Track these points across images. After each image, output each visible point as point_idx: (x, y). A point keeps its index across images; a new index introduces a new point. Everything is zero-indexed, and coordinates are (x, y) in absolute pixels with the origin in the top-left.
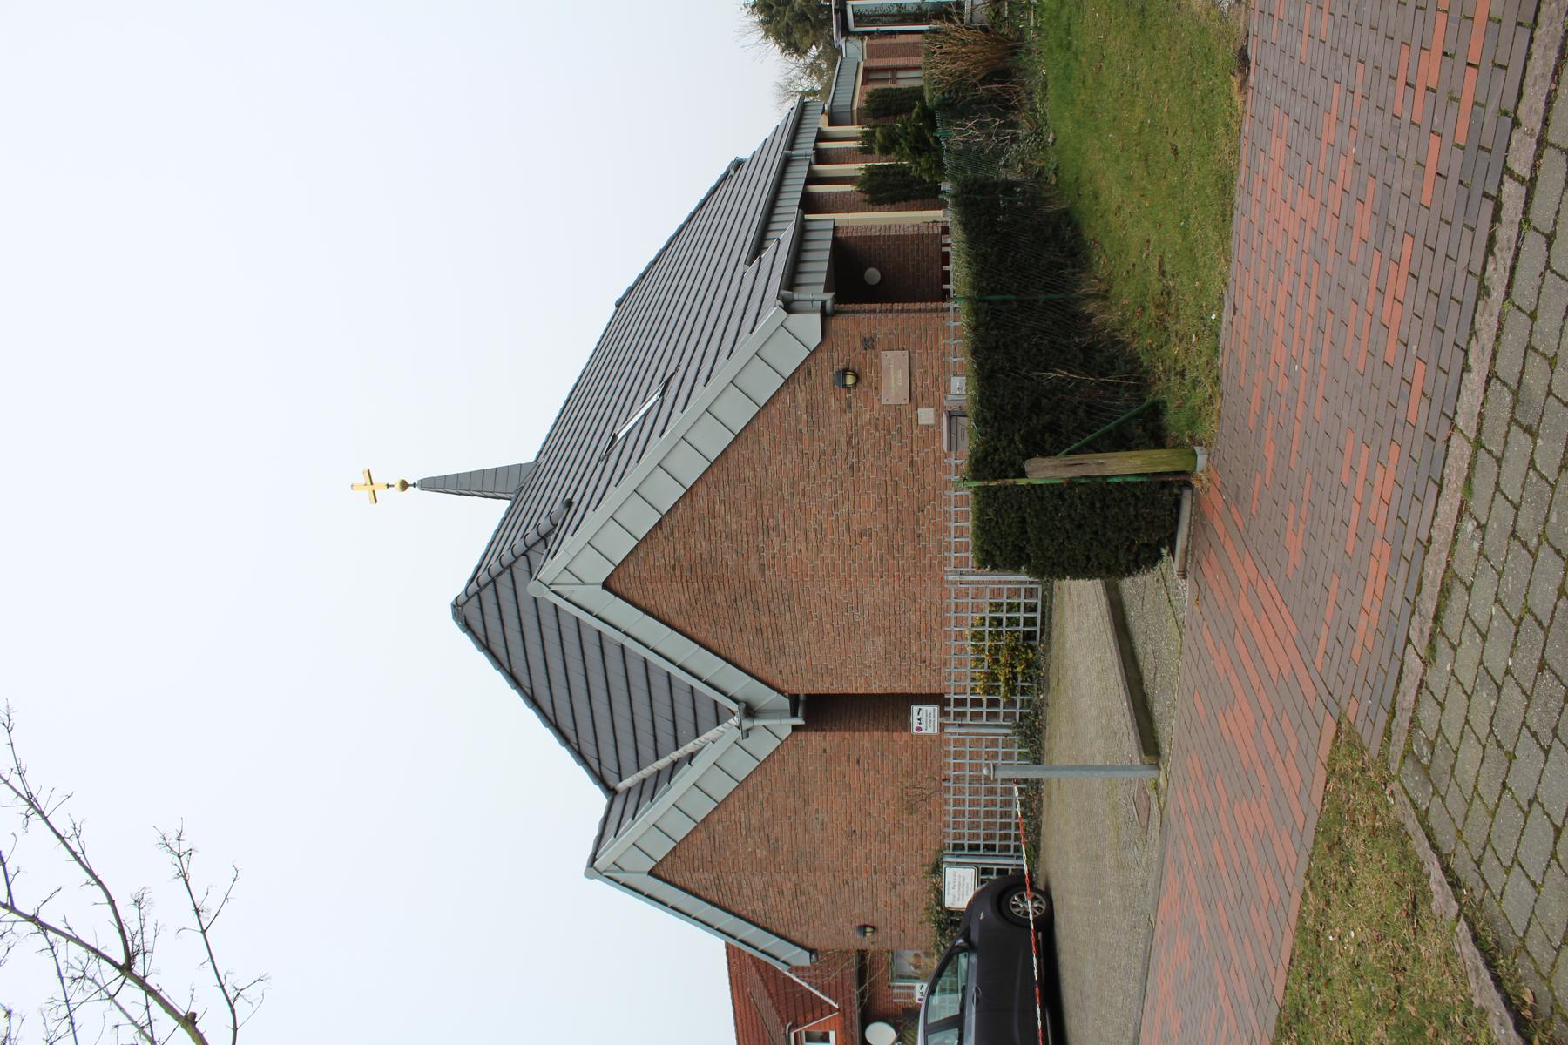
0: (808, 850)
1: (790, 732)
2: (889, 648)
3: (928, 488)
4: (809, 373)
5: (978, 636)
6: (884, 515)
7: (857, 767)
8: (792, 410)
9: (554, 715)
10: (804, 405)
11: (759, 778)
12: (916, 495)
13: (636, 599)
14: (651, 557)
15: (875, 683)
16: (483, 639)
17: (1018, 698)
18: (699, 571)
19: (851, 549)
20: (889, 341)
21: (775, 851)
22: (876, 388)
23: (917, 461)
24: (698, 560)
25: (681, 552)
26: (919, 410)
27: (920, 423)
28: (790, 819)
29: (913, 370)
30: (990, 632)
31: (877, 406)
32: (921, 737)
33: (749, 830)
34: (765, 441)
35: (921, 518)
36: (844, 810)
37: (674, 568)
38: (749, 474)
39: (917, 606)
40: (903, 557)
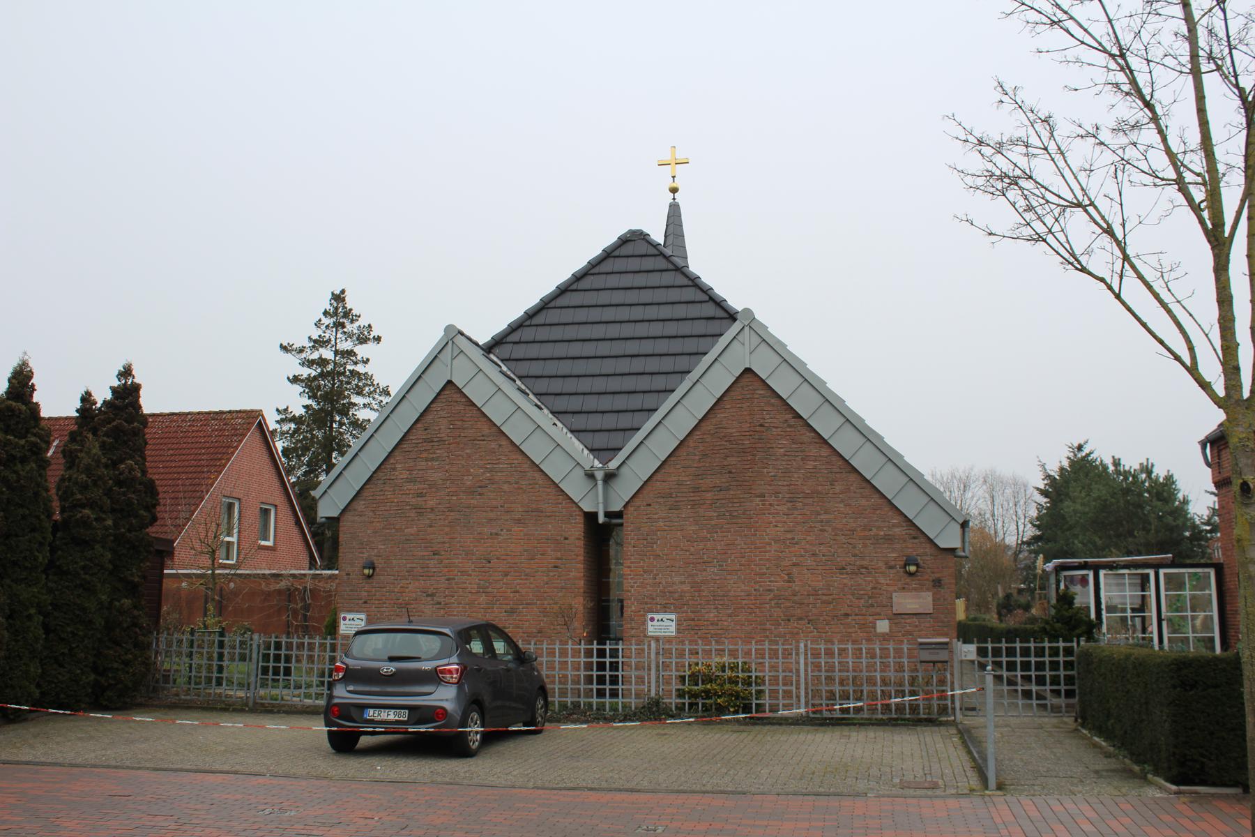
0: (471, 521)
1: (586, 510)
2: (676, 595)
3: (827, 627)
4: (914, 538)
5: (734, 668)
6: (805, 593)
7: (550, 566)
8: (887, 524)
9: (555, 308)
10: (890, 533)
11: (540, 482)
12: (822, 618)
13: (732, 393)
14: (770, 408)
15: (635, 583)
16: (616, 253)
17: (687, 701)
18: (760, 445)
19: (778, 566)
20: (939, 599)
21: (471, 491)
22: (904, 588)
23: (848, 619)
24: (769, 446)
25: (775, 432)
26: (887, 621)
27: (878, 621)
28: (501, 506)
29: (918, 616)
30: (751, 677)
31: (890, 589)
32: (644, 623)
33: (491, 471)
34: (863, 502)
35: (802, 622)
36: (510, 553)
37: (761, 425)
38: (838, 488)
39: (723, 619)
40: (771, 607)
